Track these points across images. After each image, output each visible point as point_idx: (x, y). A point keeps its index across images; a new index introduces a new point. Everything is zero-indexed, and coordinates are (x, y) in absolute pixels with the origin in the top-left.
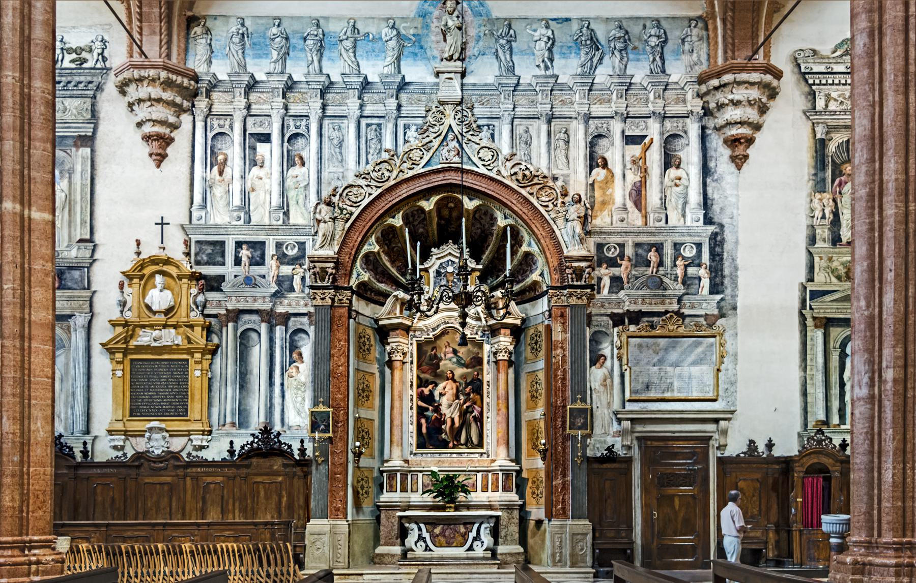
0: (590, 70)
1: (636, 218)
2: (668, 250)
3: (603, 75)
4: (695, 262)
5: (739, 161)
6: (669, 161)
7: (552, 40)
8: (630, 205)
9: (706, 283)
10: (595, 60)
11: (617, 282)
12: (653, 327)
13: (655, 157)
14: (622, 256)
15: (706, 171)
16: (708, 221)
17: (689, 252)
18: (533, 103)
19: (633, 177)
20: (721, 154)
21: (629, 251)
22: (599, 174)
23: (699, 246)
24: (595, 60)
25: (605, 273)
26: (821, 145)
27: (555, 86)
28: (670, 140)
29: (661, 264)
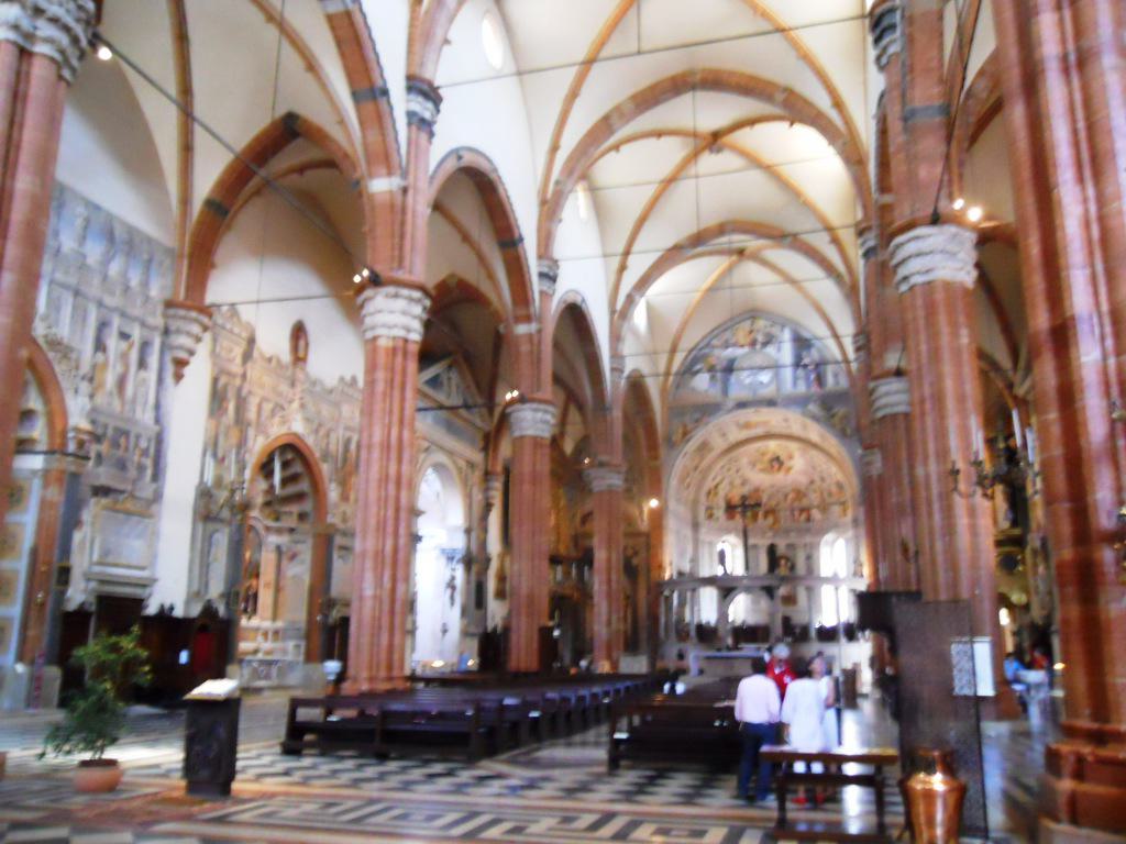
0: (106, 262)
1: (116, 404)
2: (132, 440)
3: (115, 268)
4: (145, 453)
5: (179, 377)
6: (142, 364)
7: (87, 221)
8: (115, 391)
9: (149, 472)
10: (111, 254)
11: (99, 456)
12: (116, 502)
13: (134, 356)
14: (104, 435)
15: (160, 380)
16: (158, 420)
17: (143, 444)
18: (66, 273)
19: (119, 369)
20: (170, 369)
21: (110, 432)
22: (100, 357)
23: (149, 440)
24: (111, 254)
25: (93, 449)
26: (215, 381)
27: (83, 267)
28: (145, 346)
29: (127, 449)
